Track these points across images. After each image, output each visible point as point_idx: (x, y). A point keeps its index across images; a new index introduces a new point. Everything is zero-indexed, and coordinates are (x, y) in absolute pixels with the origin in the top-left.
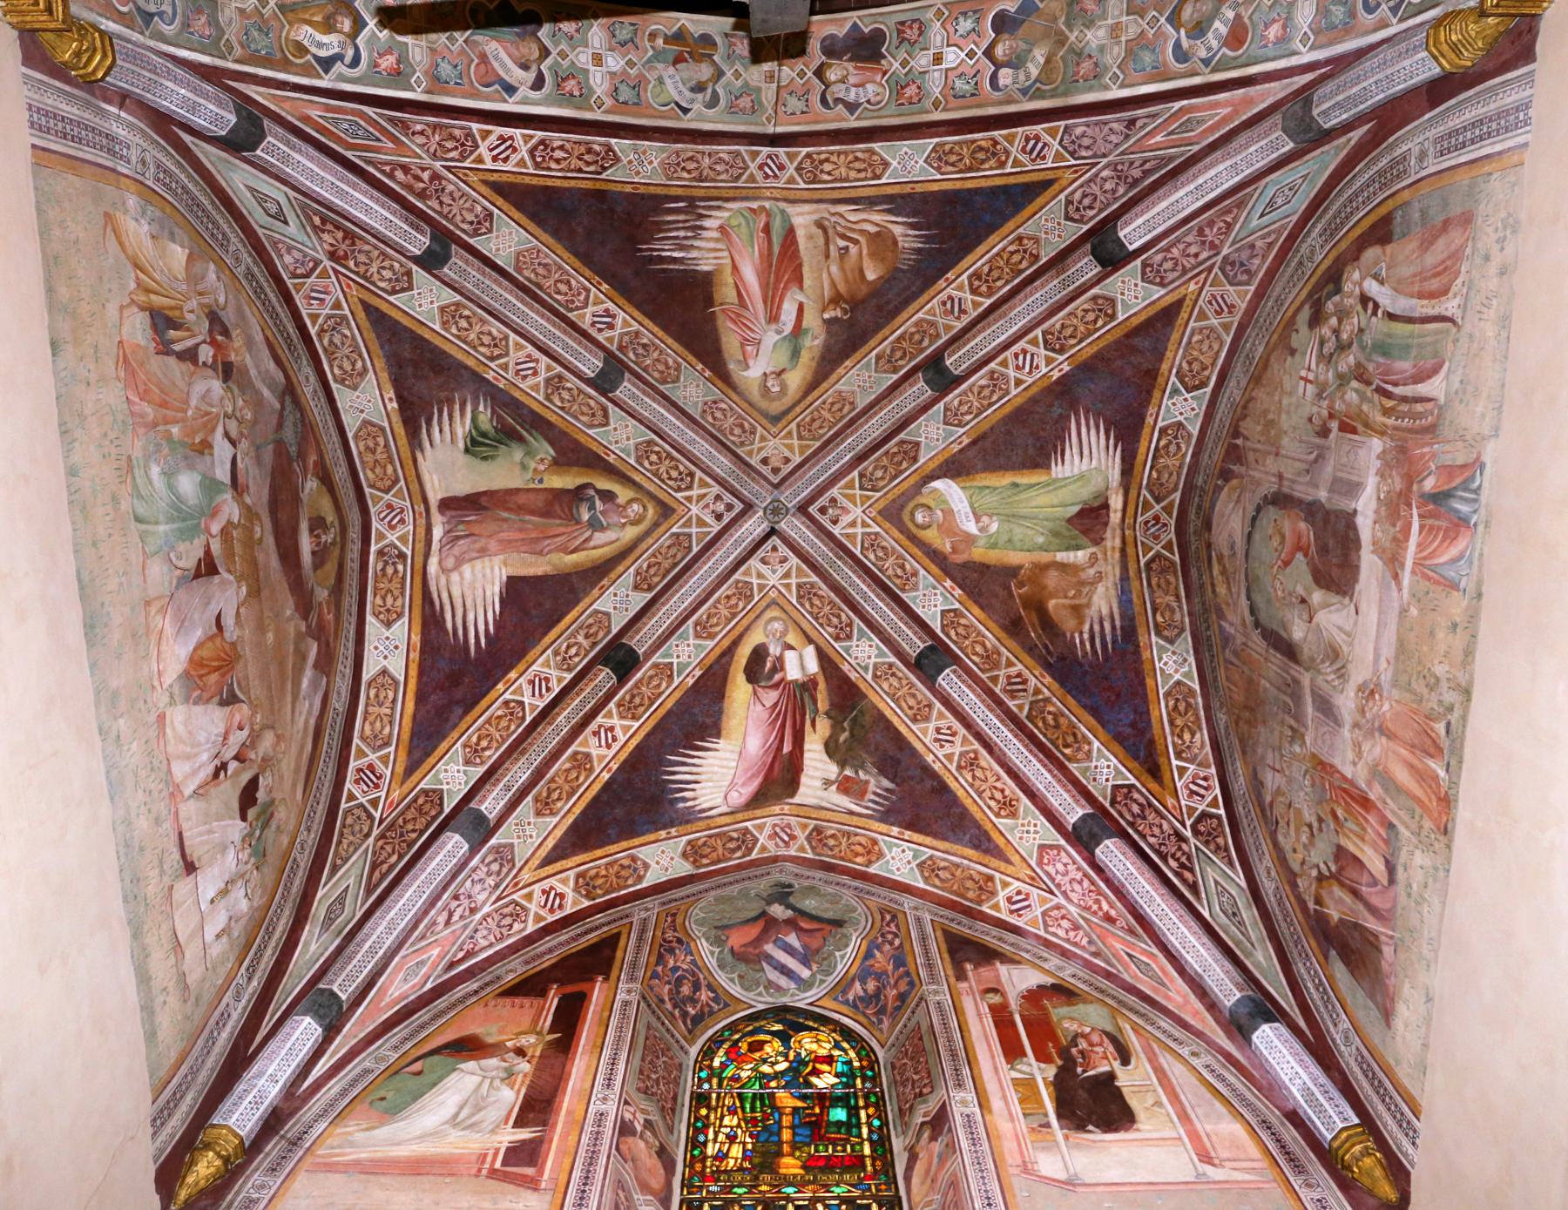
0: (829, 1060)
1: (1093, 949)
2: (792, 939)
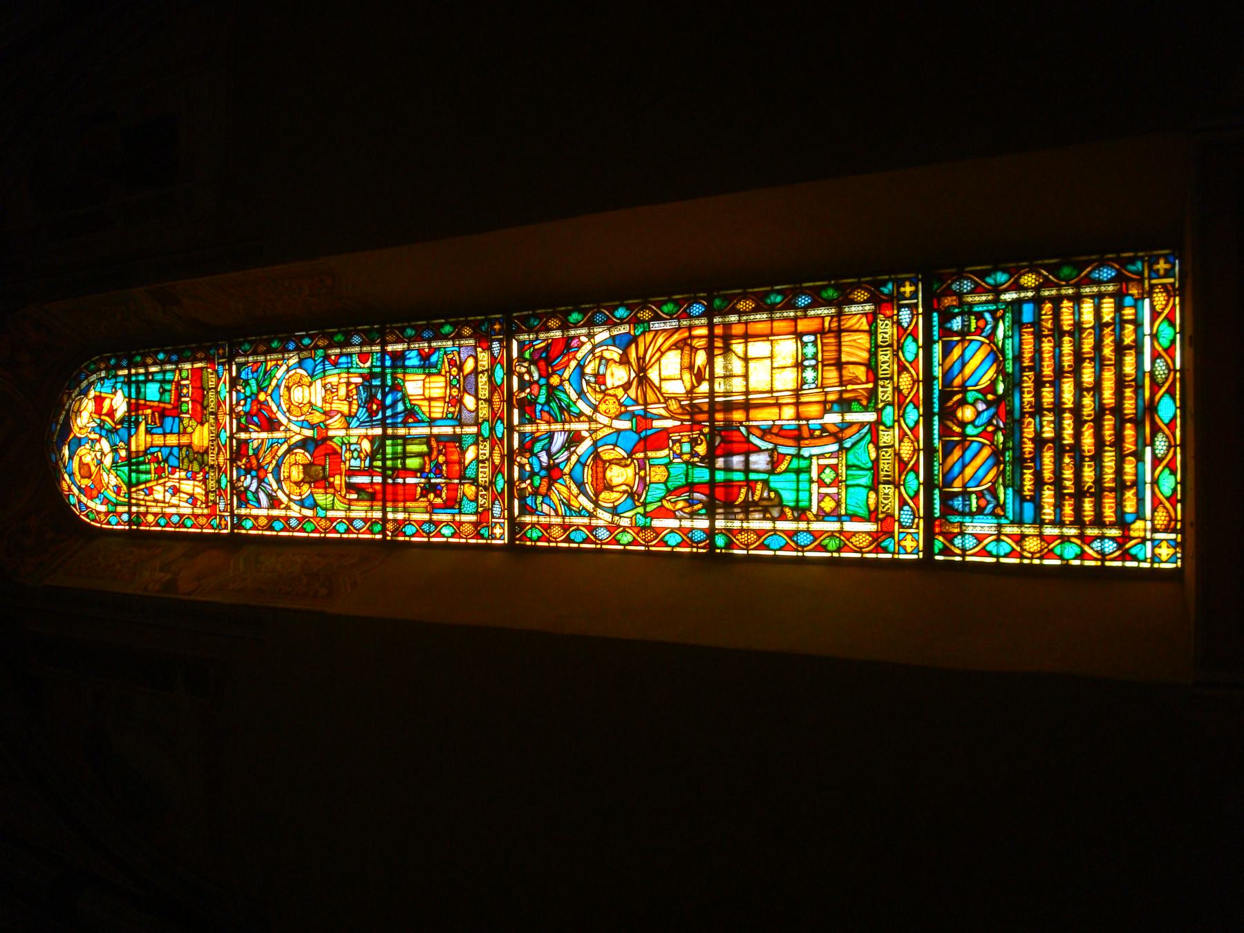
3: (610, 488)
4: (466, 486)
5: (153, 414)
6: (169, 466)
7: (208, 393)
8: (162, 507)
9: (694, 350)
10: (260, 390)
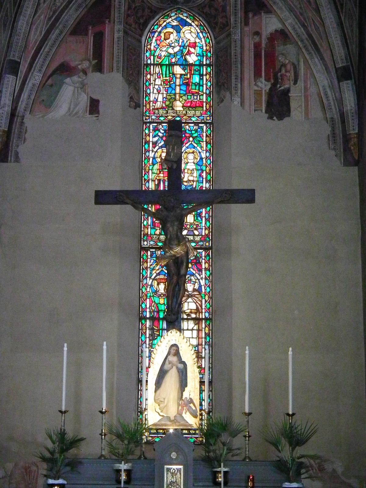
0: (194, 45)
1: (301, 11)
3: (158, 284)
4: (159, 231)
5: (188, 79)
6: (168, 88)
7: (194, 110)
8: (152, 84)
9: (196, 313)
10: (194, 138)
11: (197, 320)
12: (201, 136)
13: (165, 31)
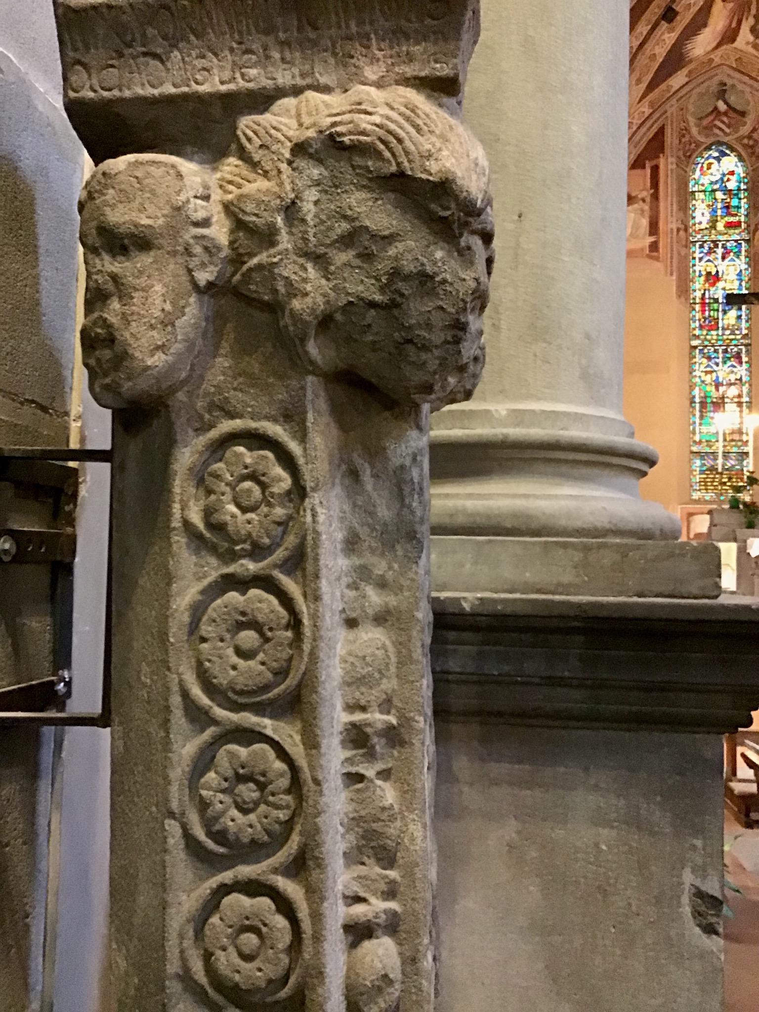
0: (732, 173)
2: (725, 119)
11: (740, 404)
12: (740, 251)
13: (707, 162)
